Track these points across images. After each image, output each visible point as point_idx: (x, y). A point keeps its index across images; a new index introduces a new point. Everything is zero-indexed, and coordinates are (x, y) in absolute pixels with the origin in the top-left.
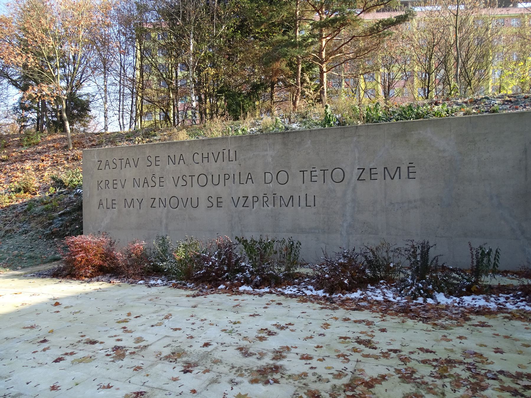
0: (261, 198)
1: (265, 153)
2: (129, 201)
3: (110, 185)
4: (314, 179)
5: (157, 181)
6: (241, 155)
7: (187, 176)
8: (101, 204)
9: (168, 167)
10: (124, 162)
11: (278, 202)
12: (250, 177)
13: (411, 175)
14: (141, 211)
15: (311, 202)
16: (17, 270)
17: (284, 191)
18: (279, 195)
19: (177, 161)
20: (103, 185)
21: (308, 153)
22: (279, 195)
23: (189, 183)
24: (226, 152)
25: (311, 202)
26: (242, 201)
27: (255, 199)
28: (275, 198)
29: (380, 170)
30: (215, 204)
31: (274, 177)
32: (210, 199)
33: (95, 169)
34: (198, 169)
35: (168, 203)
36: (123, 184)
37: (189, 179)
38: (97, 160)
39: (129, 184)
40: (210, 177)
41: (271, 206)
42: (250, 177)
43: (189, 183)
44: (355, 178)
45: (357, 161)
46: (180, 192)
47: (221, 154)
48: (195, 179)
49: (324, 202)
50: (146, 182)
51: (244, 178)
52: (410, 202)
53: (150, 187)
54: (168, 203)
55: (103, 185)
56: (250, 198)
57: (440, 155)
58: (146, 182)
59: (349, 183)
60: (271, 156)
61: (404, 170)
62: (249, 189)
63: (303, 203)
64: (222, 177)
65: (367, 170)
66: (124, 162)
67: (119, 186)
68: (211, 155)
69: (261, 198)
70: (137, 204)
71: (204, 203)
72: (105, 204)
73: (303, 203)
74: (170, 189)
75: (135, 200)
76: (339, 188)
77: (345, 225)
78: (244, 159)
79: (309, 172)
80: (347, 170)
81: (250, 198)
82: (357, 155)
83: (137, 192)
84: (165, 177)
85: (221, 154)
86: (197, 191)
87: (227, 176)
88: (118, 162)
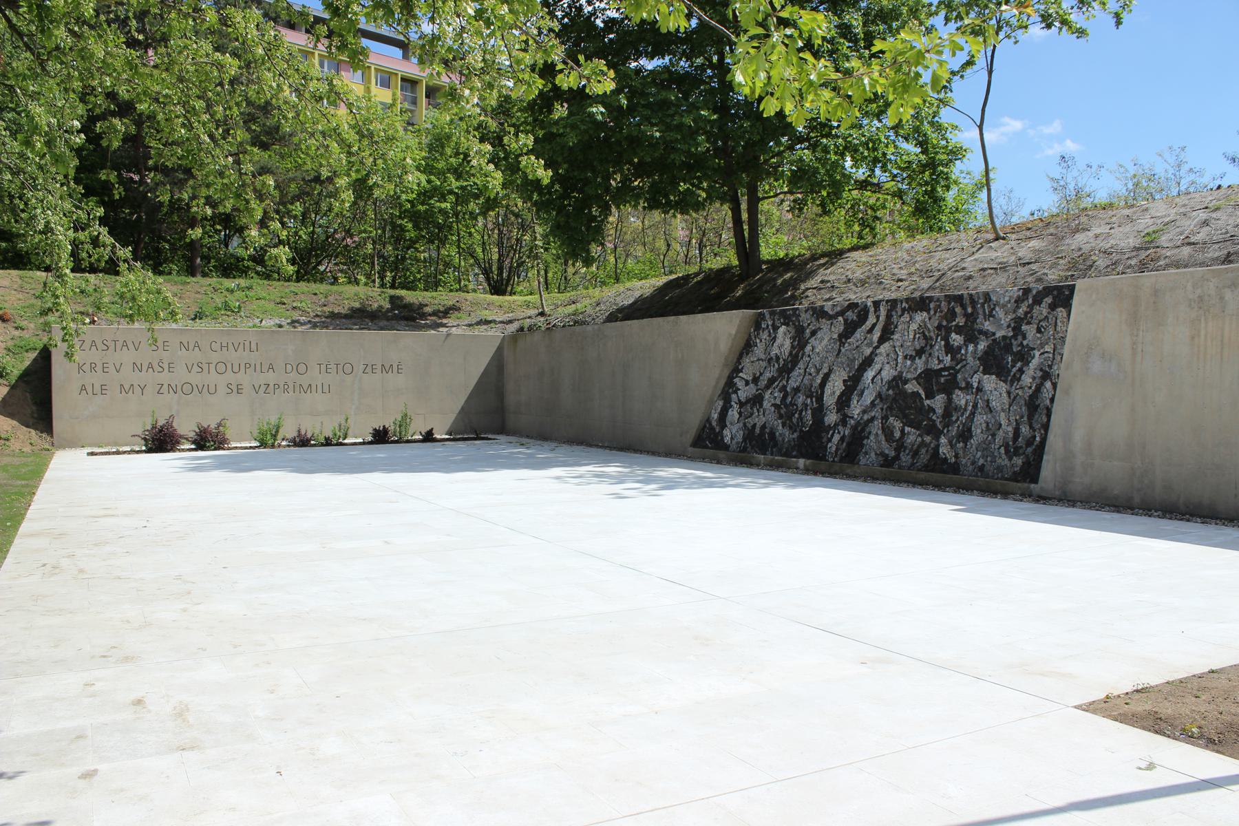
2: (127, 387)
3: (99, 368)
5: (166, 366)
8: (83, 388)
10: (119, 345)
12: (271, 367)
15: (326, 390)
16: (208, 449)
17: (304, 380)
23: (206, 370)
25: (326, 390)
26: (263, 388)
27: (277, 386)
29: (379, 367)
30: (235, 390)
34: (215, 358)
37: (205, 367)
40: (229, 366)
42: (271, 367)
43: (206, 370)
46: (195, 378)
48: (212, 367)
50: (150, 366)
58: (150, 366)
62: (271, 377)
66: (119, 345)
67: (112, 370)
68: (230, 346)
71: (223, 390)
72: (89, 389)
76: (349, 379)
86: (212, 378)
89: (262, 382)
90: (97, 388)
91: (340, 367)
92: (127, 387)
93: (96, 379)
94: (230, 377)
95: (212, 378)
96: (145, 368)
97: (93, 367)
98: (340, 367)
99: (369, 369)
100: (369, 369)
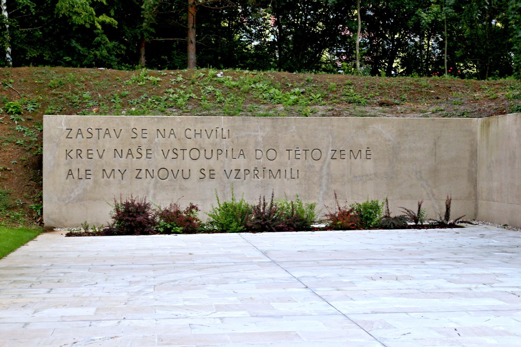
0: (252, 171)
1: (257, 134)
2: (108, 172)
3: (84, 154)
4: (298, 156)
5: (144, 152)
6: (234, 134)
8: (70, 173)
10: (102, 132)
13: (368, 157)
14: (124, 182)
17: (273, 166)
18: (268, 168)
19: (167, 134)
21: (293, 136)
22: (268, 168)
26: (234, 173)
28: (265, 171)
29: (347, 152)
30: (207, 175)
31: (265, 153)
32: (202, 171)
33: (63, 138)
34: (190, 144)
36: (101, 154)
37: (180, 152)
38: (65, 128)
39: (109, 156)
40: (202, 152)
41: (261, 178)
42: (242, 153)
44: (329, 157)
45: (330, 145)
46: (170, 164)
47: (214, 132)
49: (305, 175)
51: (236, 153)
52: (367, 175)
53: (135, 159)
54: (156, 174)
55: (73, 154)
56: (242, 171)
57: (387, 143)
59: (325, 161)
60: (262, 136)
61: (363, 152)
62: (241, 163)
63: (288, 176)
64: (215, 152)
65: (338, 151)
66: (102, 132)
67: (96, 156)
68: (203, 132)
69: (252, 171)
70: (118, 175)
71: (196, 175)
72: (75, 174)
73: (288, 176)
74: (158, 160)
75: (116, 170)
76: (317, 165)
77: (321, 192)
78: (237, 138)
79: (294, 151)
80: (323, 151)
81: (242, 171)
82: (331, 140)
83: (120, 163)
84: (153, 149)
85: (214, 132)
86: (187, 163)
88: (95, 133)
90: (82, 172)
92: (108, 172)
94: (203, 162)
96: (125, 154)
98: (309, 153)
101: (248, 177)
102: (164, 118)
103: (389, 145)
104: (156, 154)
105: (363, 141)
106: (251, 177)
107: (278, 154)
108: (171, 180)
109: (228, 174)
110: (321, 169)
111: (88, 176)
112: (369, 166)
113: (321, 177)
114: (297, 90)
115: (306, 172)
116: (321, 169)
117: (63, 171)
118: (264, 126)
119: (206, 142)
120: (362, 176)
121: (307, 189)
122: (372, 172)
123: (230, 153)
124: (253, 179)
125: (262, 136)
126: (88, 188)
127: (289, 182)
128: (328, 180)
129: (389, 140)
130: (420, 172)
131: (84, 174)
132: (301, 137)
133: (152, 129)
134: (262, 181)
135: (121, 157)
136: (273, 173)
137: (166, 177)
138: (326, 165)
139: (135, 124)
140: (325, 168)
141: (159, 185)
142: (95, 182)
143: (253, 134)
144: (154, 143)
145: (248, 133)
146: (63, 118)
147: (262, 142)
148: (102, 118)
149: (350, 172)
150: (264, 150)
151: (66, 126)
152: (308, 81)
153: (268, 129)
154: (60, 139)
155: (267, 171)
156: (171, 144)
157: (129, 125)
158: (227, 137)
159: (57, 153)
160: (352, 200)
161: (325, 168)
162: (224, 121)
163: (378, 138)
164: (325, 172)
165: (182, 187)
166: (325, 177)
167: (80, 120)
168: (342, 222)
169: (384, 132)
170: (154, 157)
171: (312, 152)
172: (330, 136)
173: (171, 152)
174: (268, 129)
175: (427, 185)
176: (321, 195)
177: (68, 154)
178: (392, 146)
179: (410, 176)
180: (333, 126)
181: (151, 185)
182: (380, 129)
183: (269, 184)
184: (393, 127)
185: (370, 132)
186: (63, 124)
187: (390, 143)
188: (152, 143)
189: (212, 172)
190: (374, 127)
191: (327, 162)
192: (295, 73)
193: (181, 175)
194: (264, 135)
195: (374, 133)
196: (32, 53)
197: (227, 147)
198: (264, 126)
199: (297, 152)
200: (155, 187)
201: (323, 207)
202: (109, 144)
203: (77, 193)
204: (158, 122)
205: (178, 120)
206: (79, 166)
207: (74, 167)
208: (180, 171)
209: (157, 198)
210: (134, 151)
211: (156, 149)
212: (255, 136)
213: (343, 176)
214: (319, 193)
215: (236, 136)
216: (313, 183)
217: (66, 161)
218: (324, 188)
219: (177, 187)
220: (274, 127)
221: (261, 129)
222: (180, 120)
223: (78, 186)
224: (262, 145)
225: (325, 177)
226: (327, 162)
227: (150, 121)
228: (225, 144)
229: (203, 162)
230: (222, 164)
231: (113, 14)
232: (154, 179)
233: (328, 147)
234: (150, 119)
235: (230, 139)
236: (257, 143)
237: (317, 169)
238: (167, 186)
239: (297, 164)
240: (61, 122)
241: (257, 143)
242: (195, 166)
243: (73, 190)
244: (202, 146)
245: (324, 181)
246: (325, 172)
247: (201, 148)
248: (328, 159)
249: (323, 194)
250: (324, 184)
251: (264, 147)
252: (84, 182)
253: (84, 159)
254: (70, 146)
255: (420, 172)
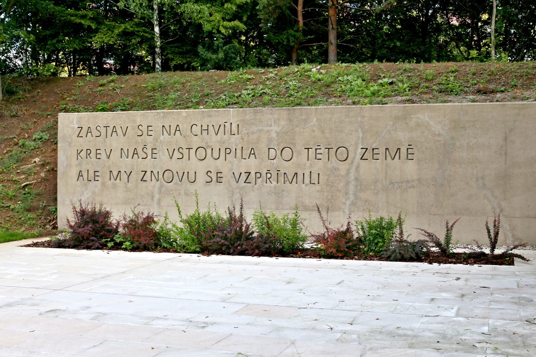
0: (264, 174)
1: (270, 128)
2: (115, 173)
3: (93, 155)
4: (319, 156)
5: (149, 152)
6: (244, 129)
7: (184, 148)
8: (80, 175)
9: (162, 138)
10: (110, 130)
11: (281, 179)
13: (410, 157)
14: (129, 185)
15: (315, 179)
17: (289, 168)
18: (282, 171)
19: (173, 131)
20: (83, 154)
21: (313, 131)
22: (282, 171)
24: (227, 125)
25: (315, 179)
26: (244, 177)
28: (279, 175)
29: (382, 150)
30: (214, 178)
31: (279, 153)
32: (209, 174)
33: (75, 137)
34: (196, 142)
35: (161, 176)
37: (186, 152)
38: (76, 126)
39: (115, 155)
40: (209, 151)
41: (274, 183)
42: (252, 153)
44: (359, 156)
45: (360, 141)
46: (175, 165)
47: (222, 127)
48: (193, 152)
49: (328, 180)
50: (135, 152)
51: (246, 153)
52: (408, 182)
53: (140, 159)
54: (161, 176)
55: (83, 154)
56: (253, 174)
57: (436, 138)
58: (135, 152)
59: (352, 162)
60: (276, 132)
61: (403, 151)
62: (252, 164)
63: (307, 180)
64: (223, 151)
65: (370, 149)
67: (103, 156)
68: (211, 128)
69: (264, 174)
70: (124, 177)
71: (202, 178)
72: (85, 176)
73: (307, 180)
74: (163, 161)
75: (122, 172)
76: (343, 167)
77: (348, 203)
78: (248, 134)
79: (314, 150)
80: (351, 149)
81: (253, 174)
82: (361, 135)
84: (158, 148)
85: (222, 127)
86: (193, 165)
87: (228, 151)
88: (103, 130)
89: (243, 170)
91: (333, 152)
93: (90, 165)
94: (210, 164)
95: (193, 165)
97: (89, 153)
98: (333, 152)
99: (368, 155)
100: (368, 155)
101: (259, 181)
102: (170, 113)
103: (439, 141)
104: (161, 154)
105: (403, 137)
106: (262, 181)
107: (294, 154)
108: (175, 184)
109: (237, 177)
110: (348, 172)
111: (97, 178)
112: (410, 169)
113: (348, 183)
114: (386, 80)
115: (329, 176)
116: (348, 172)
117: (74, 173)
118: (279, 119)
119: (213, 140)
120: (402, 182)
121: (329, 197)
122: (415, 177)
123: (239, 152)
124: (265, 184)
125: (276, 132)
126: (97, 190)
127: (307, 188)
128: (356, 186)
129: (439, 135)
130: (483, 178)
131: (93, 175)
132: (323, 132)
133: (157, 125)
134: (275, 187)
135: (127, 158)
136: (289, 177)
137: (171, 180)
138: (354, 168)
139: (141, 121)
140: (353, 171)
141: (164, 189)
142: (103, 184)
143: (266, 129)
144: (159, 141)
145: (260, 128)
146: (74, 116)
147: (276, 139)
148: (109, 115)
149: (386, 177)
150: (279, 149)
151: (77, 124)
152: (405, 70)
153: (283, 123)
154: (72, 139)
155: (281, 175)
156: (177, 141)
157: (134, 121)
158: (236, 133)
159: (69, 153)
160: (350, 218)
161: (353, 171)
162: (233, 114)
163: (423, 132)
164: (352, 176)
165: (187, 192)
166: (353, 183)
167: (90, 117)
168: (342, 247)
169: (432, 123)
170: (160, 157)
171: (337, 151)
172: (360, 130)
173: (176, 151)
174: (283, 123)
175: (493, 196)
176: (348, 205)
177: (78, 154)
178: (442, 142)
179: (467, 184)
180: (363, 117)
181: (156, 189)
182: (427, 119)
183: (283, 190)
184: (445, 117)
185: (412, 123)
186: (75, 122)
187: (439, 139)
188: (157, 141)
189: (219, 175)
190: (418, 117)
191: (355, 164)
192: (398, 63)
193: (187, 178)
194: (278, 131)
195: (418, 125)
196: (178, 61)
197: (236, 145)
198: (279, 119)
199: (318, 151)
200: (160, 192)
201: (312, 228)
202: (116, 142)
203: (86, 196)
204: (164, 117)
205: (184, 114)
206: (88, 167)
207: (84, 169)
208: (186, 174)
209: (162, 204)
210: (140, 150)
211: (161, 148)
212: (268, 131)
213: (376, 182)
214: (344, 204)
215: (247, 131)
216: (337, 190)
217: (77, 162)
218: (352, 197)
219: (183, 192)
220: (290, 120)
221: (275, 123)
222: (186, 115)
223: (87, 189)
224: (276, 143)
225: (353, 183)
226: (355, 164)
227: (156, 117)
228: (234, 142)
229: (210, 164)
230: (231, 165)
231: (245, 19)
232: (159, 182)
233: (356, 144)
234: (155, 114)
235: (240, 135)
236: (270, 140)
237: (343, 172)
238: (172, 190)
239: (318, 166)
240: (73, 120)
241: (270, 140)
242: (201, 168)
243: (83, 192)
244: (209, 144)
245: (352, 188)
246: (352, 176)
247: (208, 146)
248: (356, 160)
249: (350, 205)
250: (351, 192)
251: (278, 145)
252: (93, 183)
253: (93, 160)
254: (80, 145)
255: (483, 178)
